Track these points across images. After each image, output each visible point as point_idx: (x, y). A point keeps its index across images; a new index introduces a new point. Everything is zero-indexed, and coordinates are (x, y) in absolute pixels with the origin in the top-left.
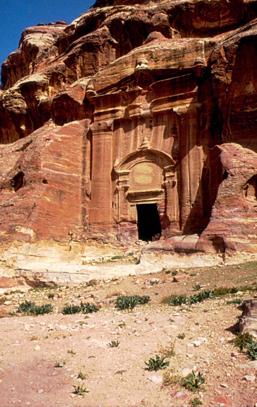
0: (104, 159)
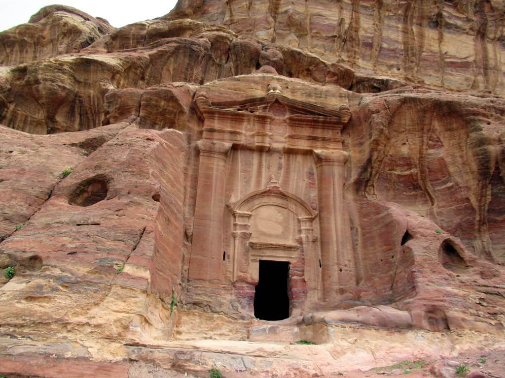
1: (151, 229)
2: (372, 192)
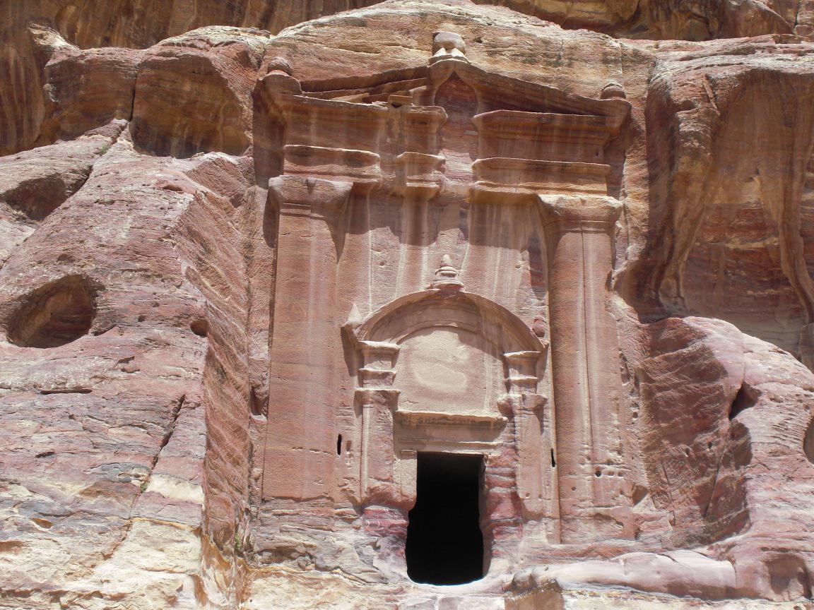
0: (317, 293)
1: (197, 400)
2: (674, 291)
